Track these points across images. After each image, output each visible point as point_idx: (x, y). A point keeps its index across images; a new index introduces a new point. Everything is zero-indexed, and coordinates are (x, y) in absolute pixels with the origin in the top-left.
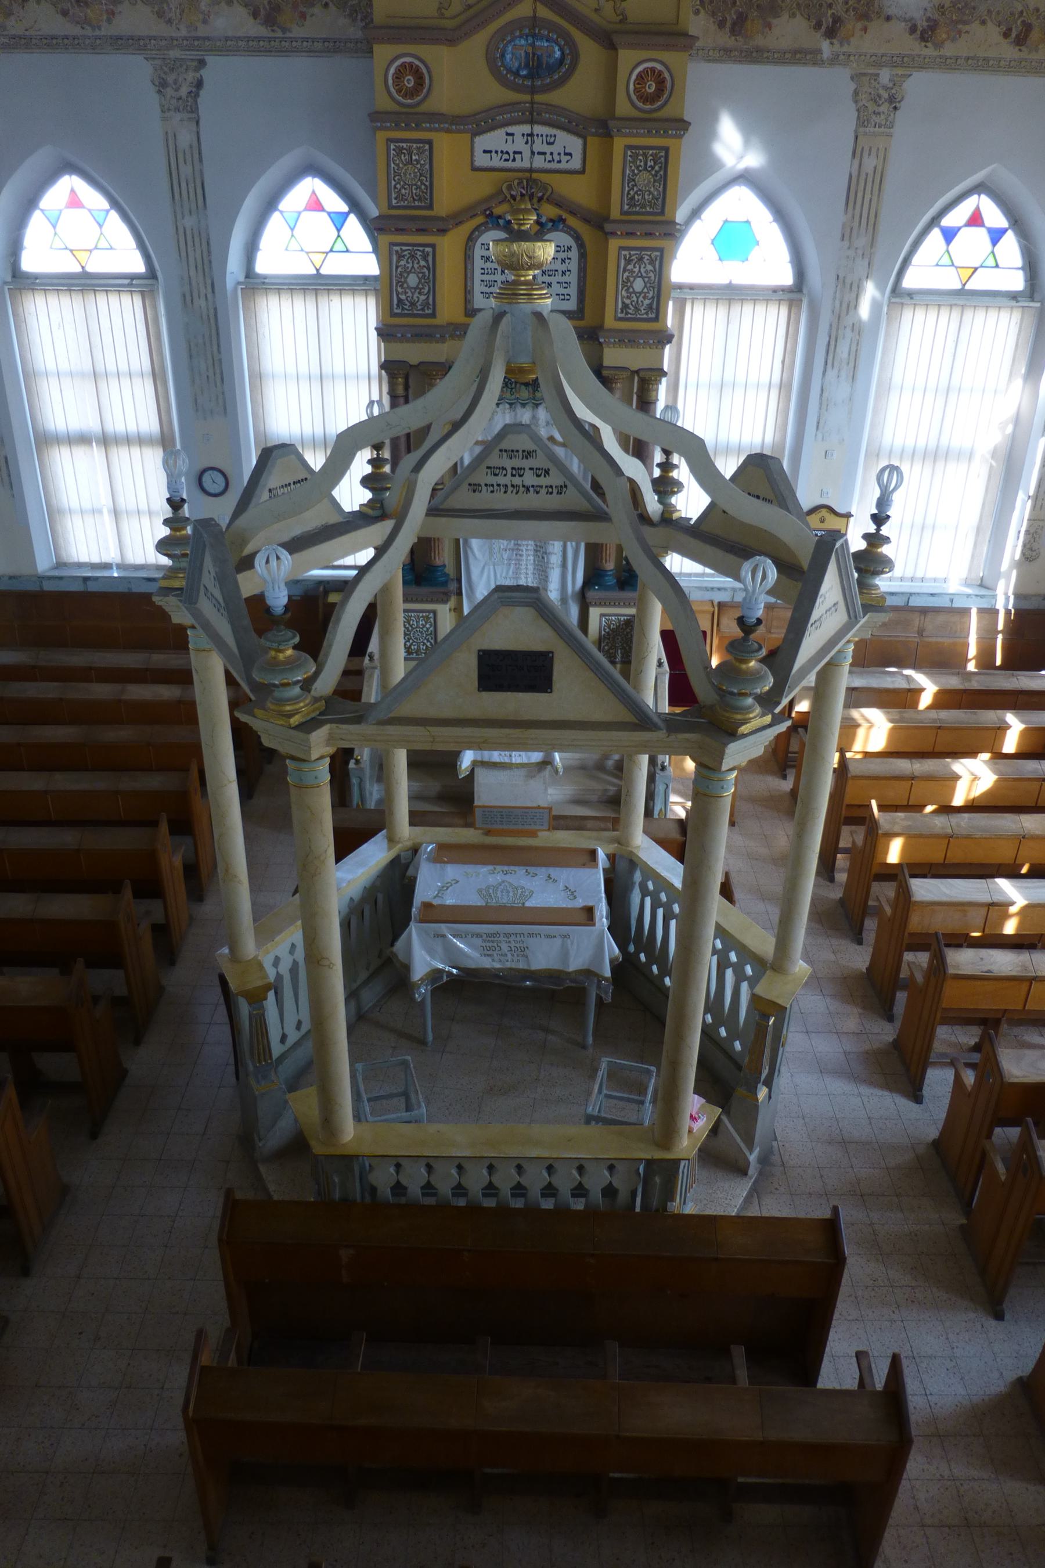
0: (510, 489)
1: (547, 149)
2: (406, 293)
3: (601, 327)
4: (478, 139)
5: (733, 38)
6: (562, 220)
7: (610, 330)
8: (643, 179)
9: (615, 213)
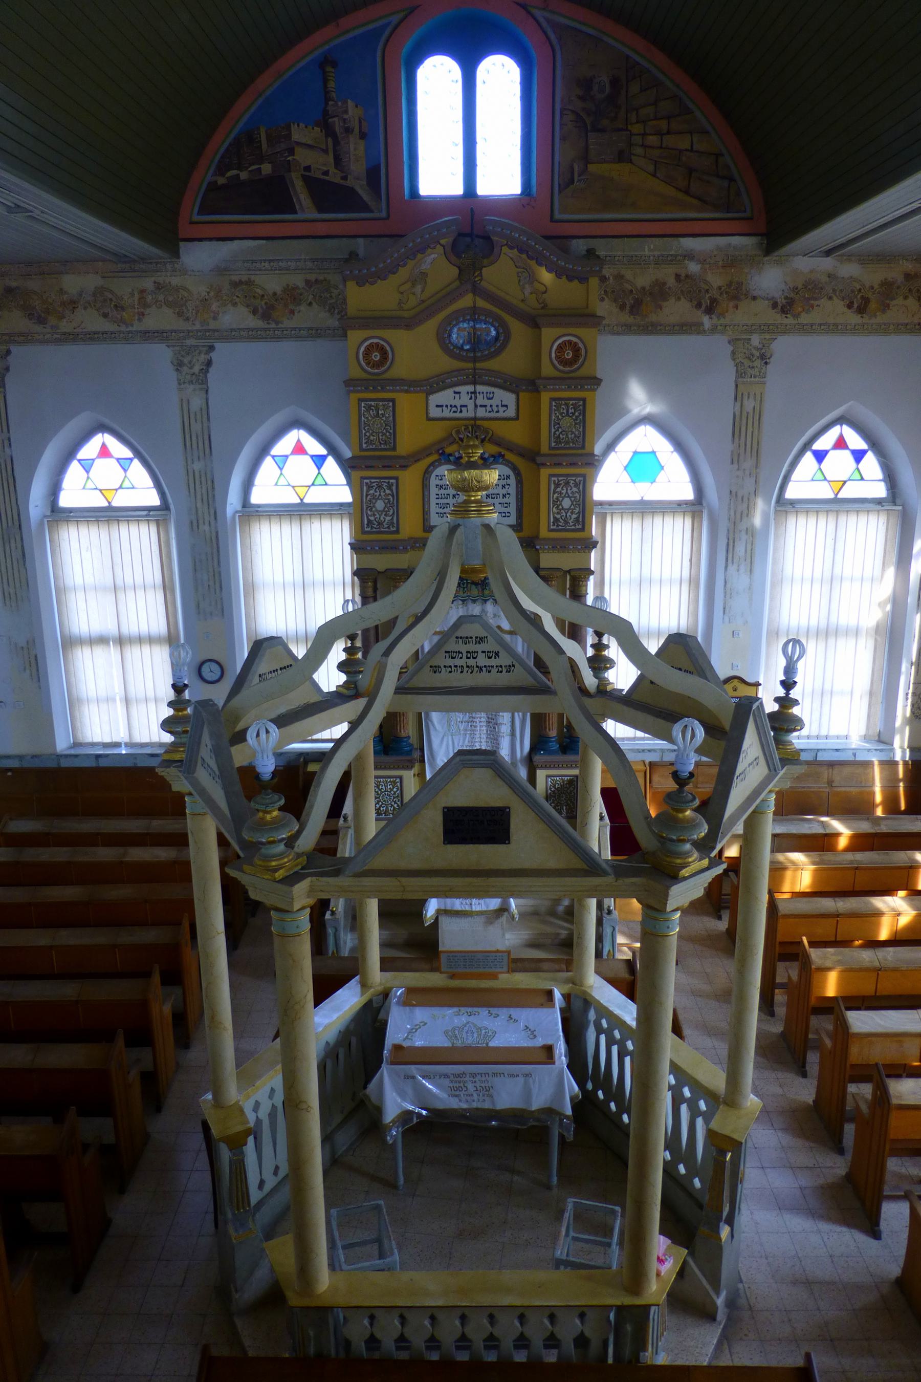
0: (466, 669)
1: (488, 402)
2: (374, 515)
3: (537, 537)
4: (431, 397)
6: (503, 456)
7: (544, 539)
8: (566, 422)
9: (544, 449)
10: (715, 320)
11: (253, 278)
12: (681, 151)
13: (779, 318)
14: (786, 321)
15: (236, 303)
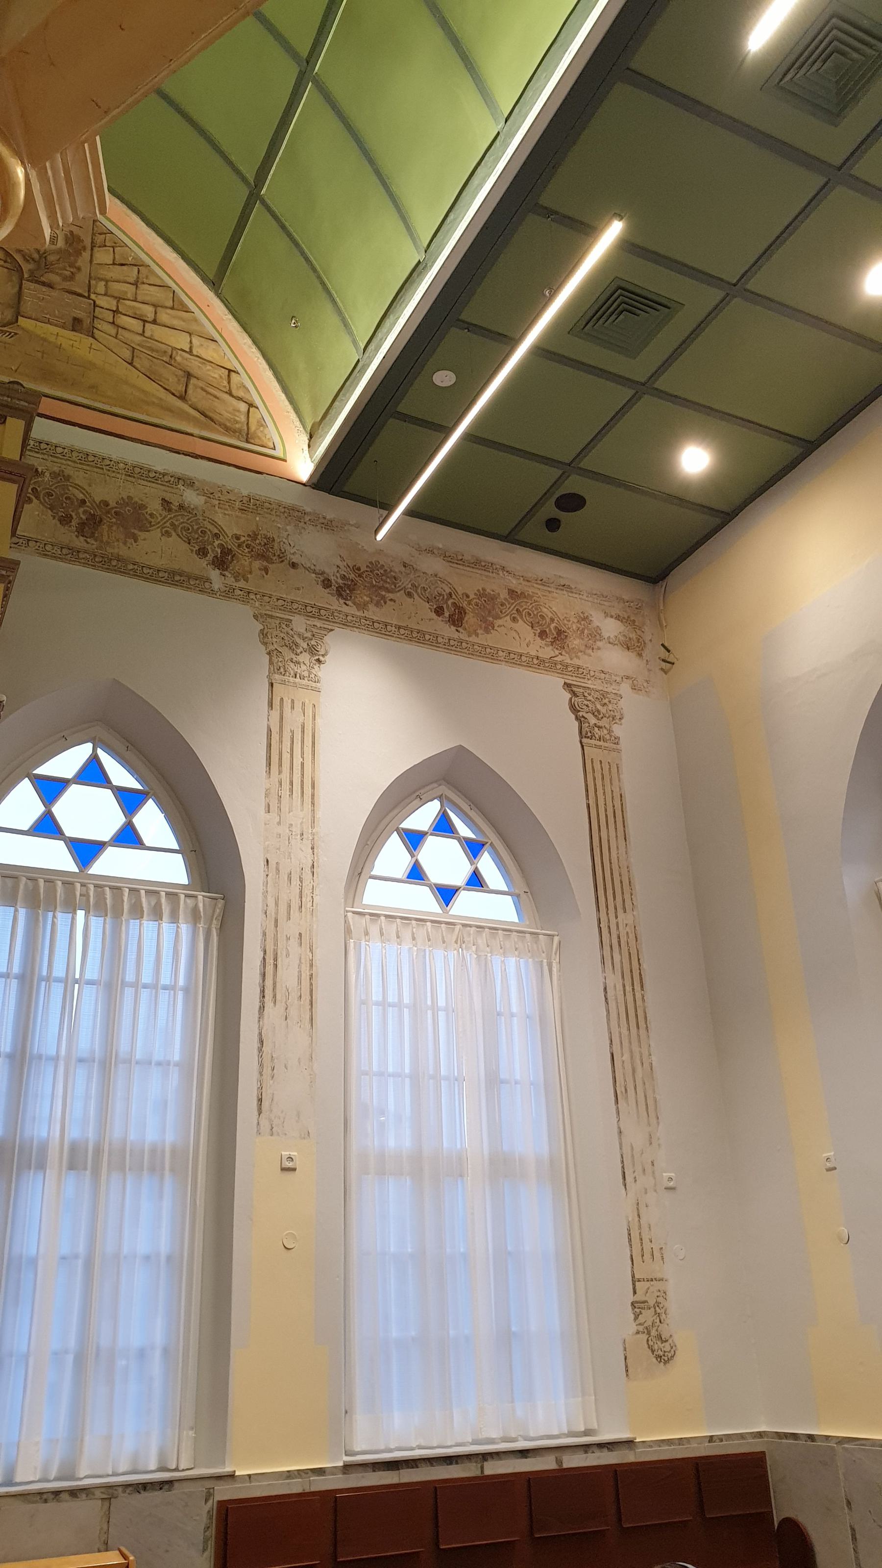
5: (82, 539)
10: (230, 580)
12: (174, 348)
13: (336, 604)
14: (345, 609)
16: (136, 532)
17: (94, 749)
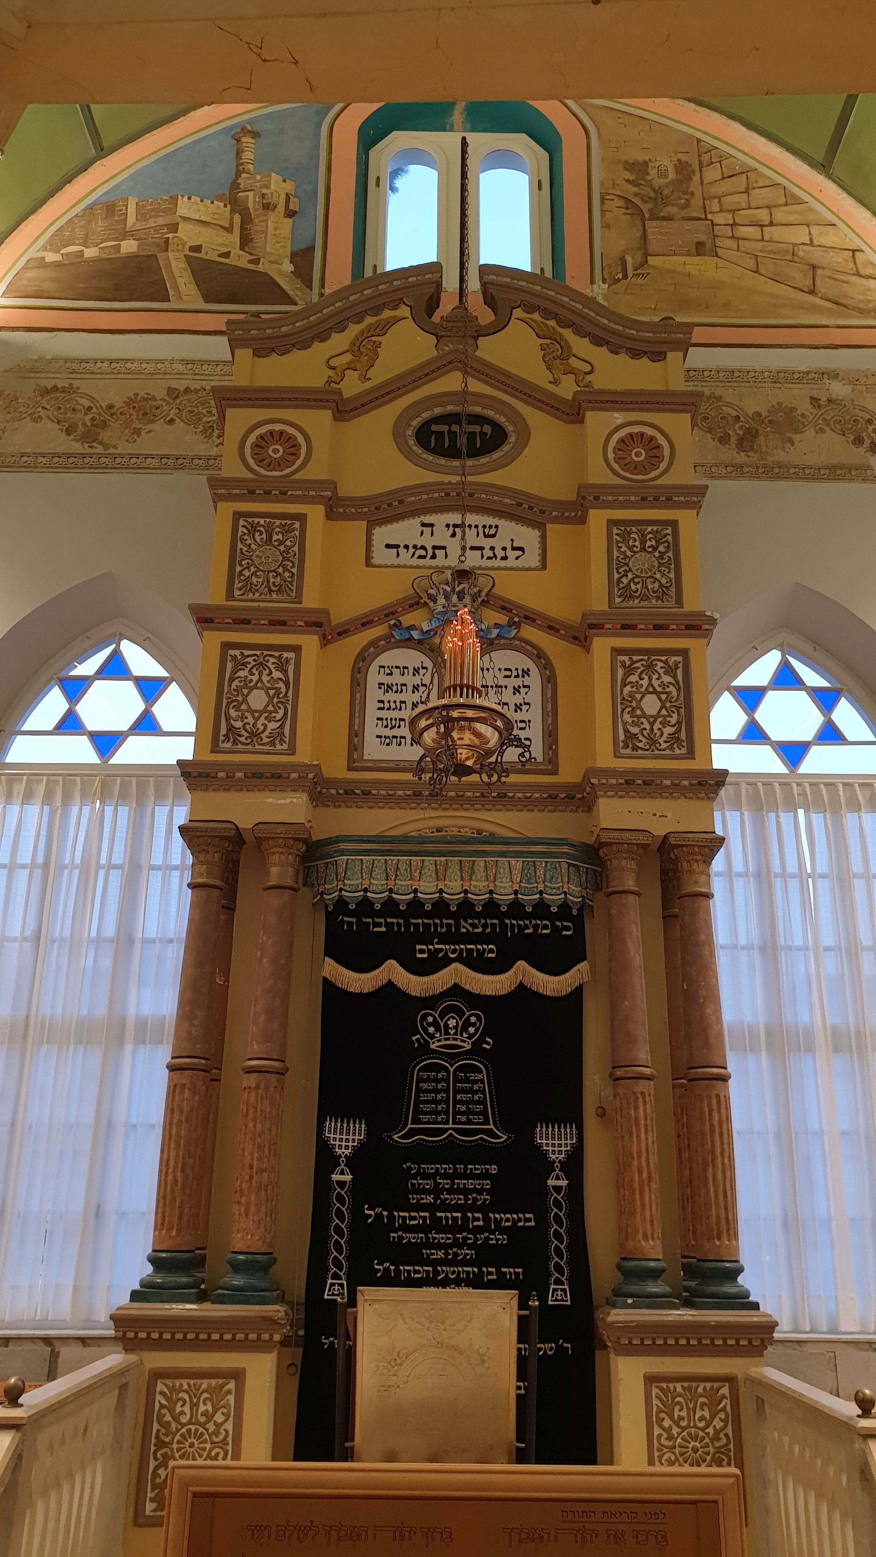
1: (487, 543)
4: (377, 531)
5: (743, 454)
8: (641, 562)
11: (76, 383)
12: (794, 245)
15: (40, 417)
16: (792, 435)
17: (783, 656)
